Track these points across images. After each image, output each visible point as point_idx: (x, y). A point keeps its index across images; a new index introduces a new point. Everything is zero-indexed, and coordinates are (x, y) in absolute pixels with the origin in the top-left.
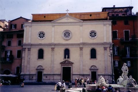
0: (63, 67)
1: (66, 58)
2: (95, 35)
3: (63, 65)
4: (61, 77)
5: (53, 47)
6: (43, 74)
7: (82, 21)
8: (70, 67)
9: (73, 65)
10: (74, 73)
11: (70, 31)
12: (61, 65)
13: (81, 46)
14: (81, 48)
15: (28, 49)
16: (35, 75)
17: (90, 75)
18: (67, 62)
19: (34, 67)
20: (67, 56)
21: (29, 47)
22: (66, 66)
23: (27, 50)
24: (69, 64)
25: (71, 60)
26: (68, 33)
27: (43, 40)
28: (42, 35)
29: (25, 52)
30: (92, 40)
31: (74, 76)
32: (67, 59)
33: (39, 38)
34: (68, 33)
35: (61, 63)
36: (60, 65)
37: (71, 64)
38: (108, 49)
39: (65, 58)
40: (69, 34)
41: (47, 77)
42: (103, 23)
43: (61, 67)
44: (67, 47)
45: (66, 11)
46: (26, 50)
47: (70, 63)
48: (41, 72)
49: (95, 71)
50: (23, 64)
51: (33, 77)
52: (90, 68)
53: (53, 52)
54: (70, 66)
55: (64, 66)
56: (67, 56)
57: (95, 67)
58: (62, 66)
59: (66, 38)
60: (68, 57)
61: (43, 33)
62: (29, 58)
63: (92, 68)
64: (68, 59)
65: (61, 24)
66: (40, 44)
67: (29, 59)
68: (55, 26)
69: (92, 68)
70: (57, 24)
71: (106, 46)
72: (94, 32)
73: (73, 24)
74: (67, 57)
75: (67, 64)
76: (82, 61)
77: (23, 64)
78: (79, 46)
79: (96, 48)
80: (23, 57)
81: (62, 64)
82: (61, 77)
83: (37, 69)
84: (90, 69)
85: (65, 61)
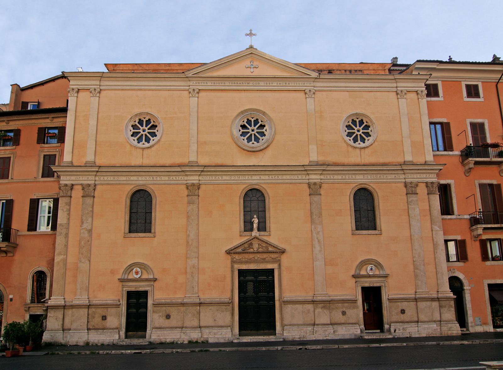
1: (251, 230)
2: (368, 135)
3: (241, 262)
4: (233, 314)
5: (194, 179)
6: (150, 302)
10: (287, 296)
11: (264, 113)
12: (233, 262)
13: (315, 178)
14: (315, 184)
15: (84, 187)
16: (118, 306)
18: (256, 246)
19: (113, 272)
20: (256, 221)
21: (89, 180)
22: (252, 267)
23: (77, 193)
26: (256, 122)
27: (146, 152)
28: (144, 130)
30: (358, 151)
31: (288, 309)
32: (255, 233)
33: (133, 141)
34: (256, 122)
35: (229, 252)
36: (227, 260)
37: (273, 256)
38: (422, 190)
39: (248, 226)
40: (262, 126)
41: (168, 317)
42: (395, 85)
43: (232, 267)
44: (254, 180)
45: (247, 35)
46: (74, 194)
47: (270, 249)
48: (145, 294)
50: (62, 257)
51: (104, 318)
54: (269, 266)
55: (244, 267)
56: (256, 221)
57: (378, 265)
58: (237, 267)
60: (262, 227)
61: (148, 122)
62: (90, 231)
63: (363, 272)
64: (262, 233)
65: (228, 85)
67: (86, 235)
68: (202, 94)
69: (368, 269)
70: (209, 85)
71: (413, 178)
72: (361, 122)
73: (275, 85)
74: (255, 226)
76: (319, 241)
77: (62, 257)
78: (303, 178)
79: (374, 186)
81: (237, 257)
82: (233, 314)
83: (121, 280)
85: (249, 243)
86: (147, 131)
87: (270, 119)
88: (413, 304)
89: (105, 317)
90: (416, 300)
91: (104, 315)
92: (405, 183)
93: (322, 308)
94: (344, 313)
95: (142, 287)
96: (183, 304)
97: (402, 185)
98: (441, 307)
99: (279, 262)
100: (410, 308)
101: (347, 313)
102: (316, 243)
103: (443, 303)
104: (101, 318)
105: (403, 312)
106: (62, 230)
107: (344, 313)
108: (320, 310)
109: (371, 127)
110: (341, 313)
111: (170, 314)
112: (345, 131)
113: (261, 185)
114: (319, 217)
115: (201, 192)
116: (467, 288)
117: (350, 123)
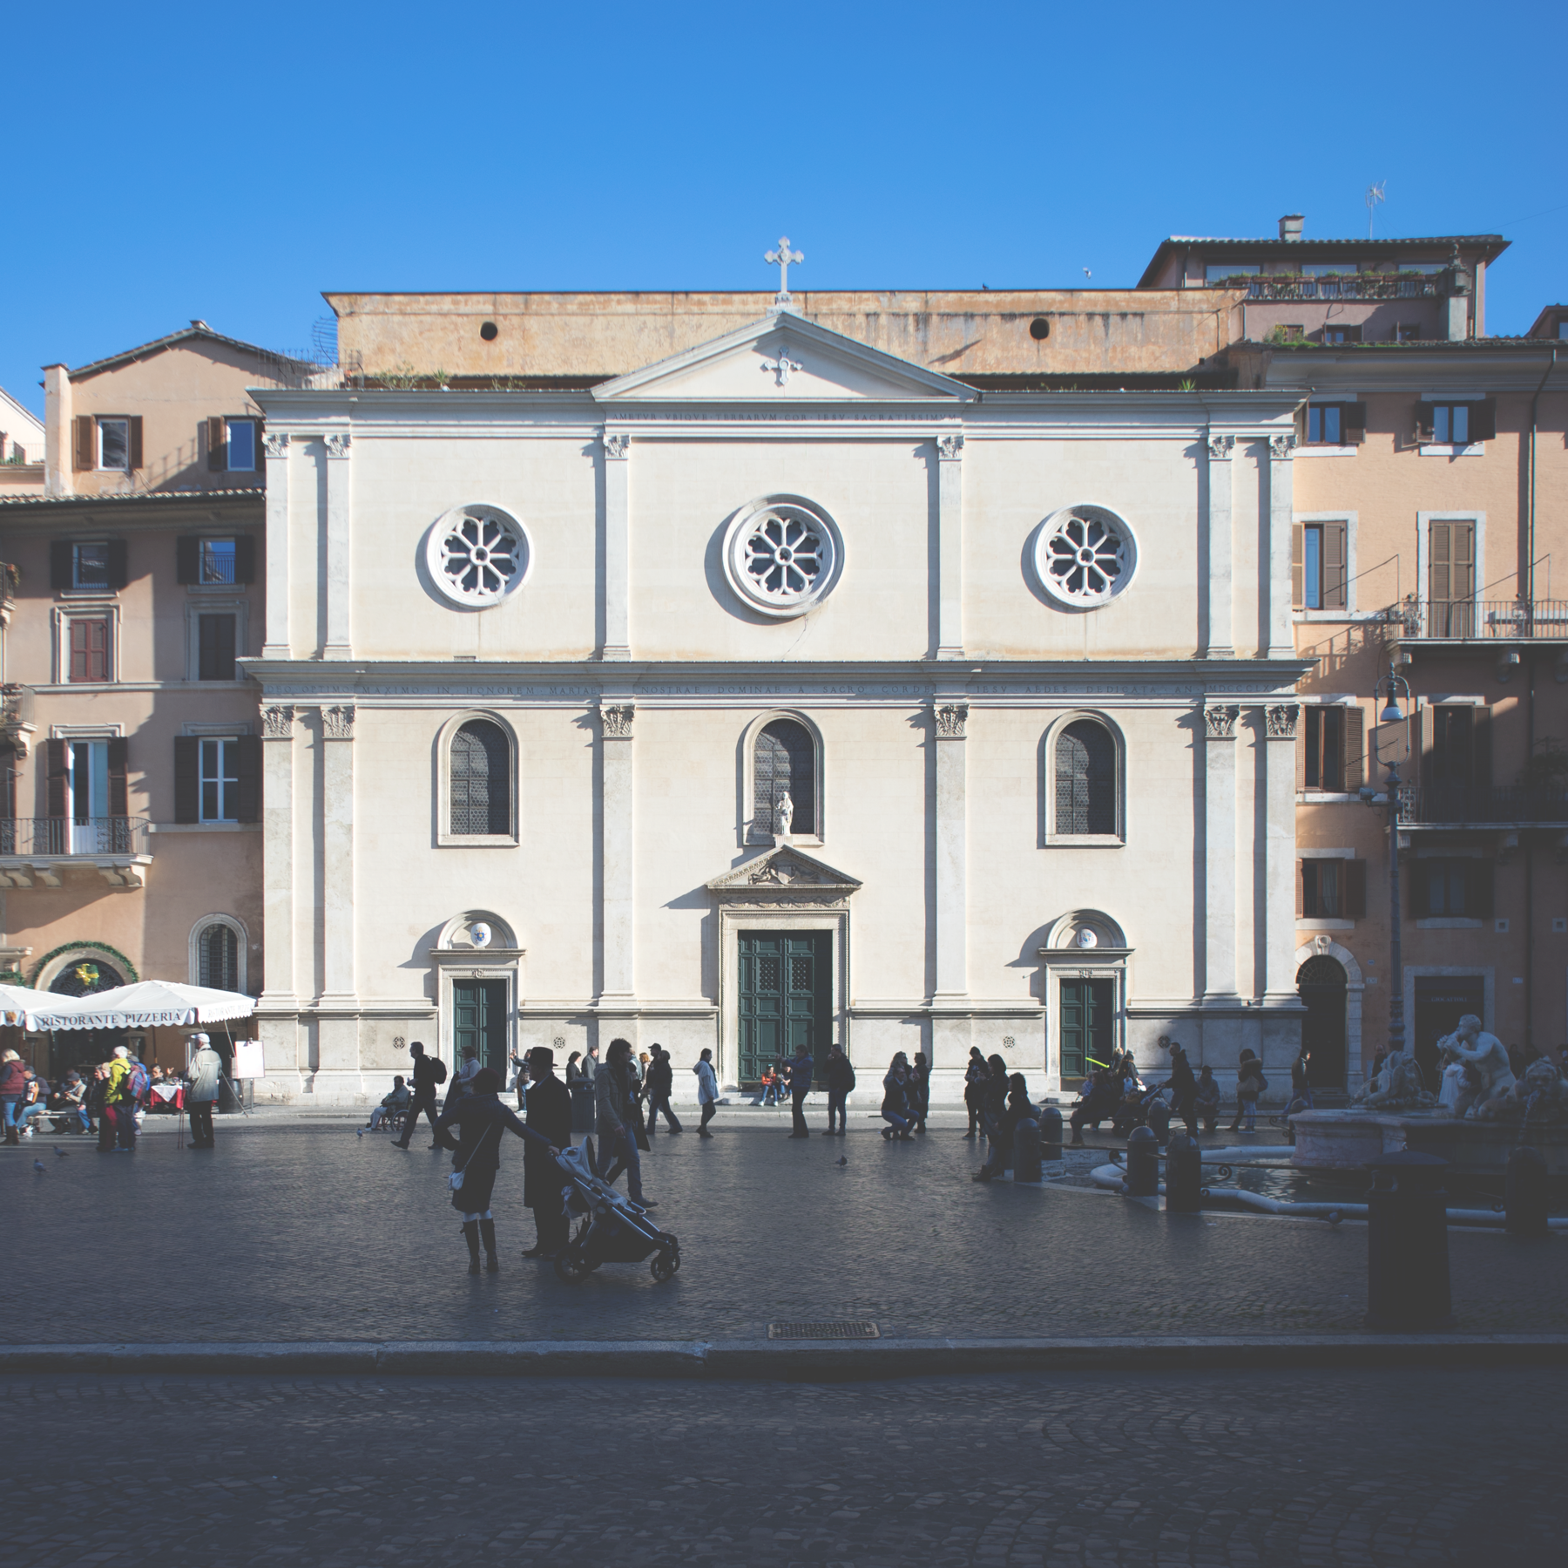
0: (743, 935)
8: (828, 934)
25: (830, 851)
49: (1100, 971)
59: (776, 597)
60: (806, 822)
80: (273, 812)
86: (490, 556)
89: (396, 1040)
91: (399, 1035)
93: (952, 1029)
101: (1017, 1042)
104: (392, 1043)
106: (277, 824)
108: (947, 1033)
109: (1122, 544)
110: (1001, 1043)
111: (564, 1037)
112: (1048, 557)
113: (805, 712)
114: (958, 799)
116: (1356, 986)
117: (1064, 535)
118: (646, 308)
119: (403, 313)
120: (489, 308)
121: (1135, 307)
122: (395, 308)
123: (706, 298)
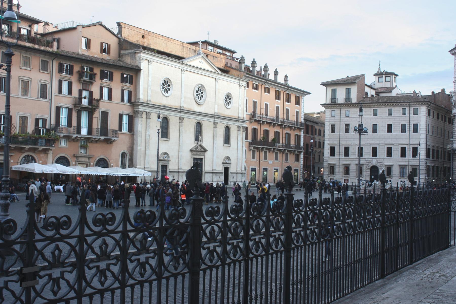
6: (168, 171)
7: (220, 72)
8: (202, 159)
9: (207, 154)
11: (204, 87)
17: (222, 173)
23: (144, 116)
24: (202, 153)
29: (142, 121)
31: (207, 175)
35: (191, 151)
38: (241, 129)
39: (197, 139)
43: (191, 157)
48: (166, 166)
52: (222, 161)
53: (182, 126)
55: (195, 157)
62: (149, 135)
66: (164, 106)
73: (208, 73)
75: (199, 153)
78: (212, 119)
80: (140, 131)
81: (193, 152)
84: (223, 163)
87: (205, 90)
88: (236, 175)
90: (237, 173)
92: (238, 126)
94: (220, 177)
95: (166, 163)
96: (178, 172)
97: (237, 126)
98: (242, 176)
99: (204, 156)
100: (235, 175)
102: (214, 148)
103: (243, 175)
105: (233, 177)
107: (220, 177)
115: (184, 121)
118: (164, 39)
119: (131, 30)
120: (143, 33)
121: (216, 56)
122: (130, 28)
123: (171, 39)
